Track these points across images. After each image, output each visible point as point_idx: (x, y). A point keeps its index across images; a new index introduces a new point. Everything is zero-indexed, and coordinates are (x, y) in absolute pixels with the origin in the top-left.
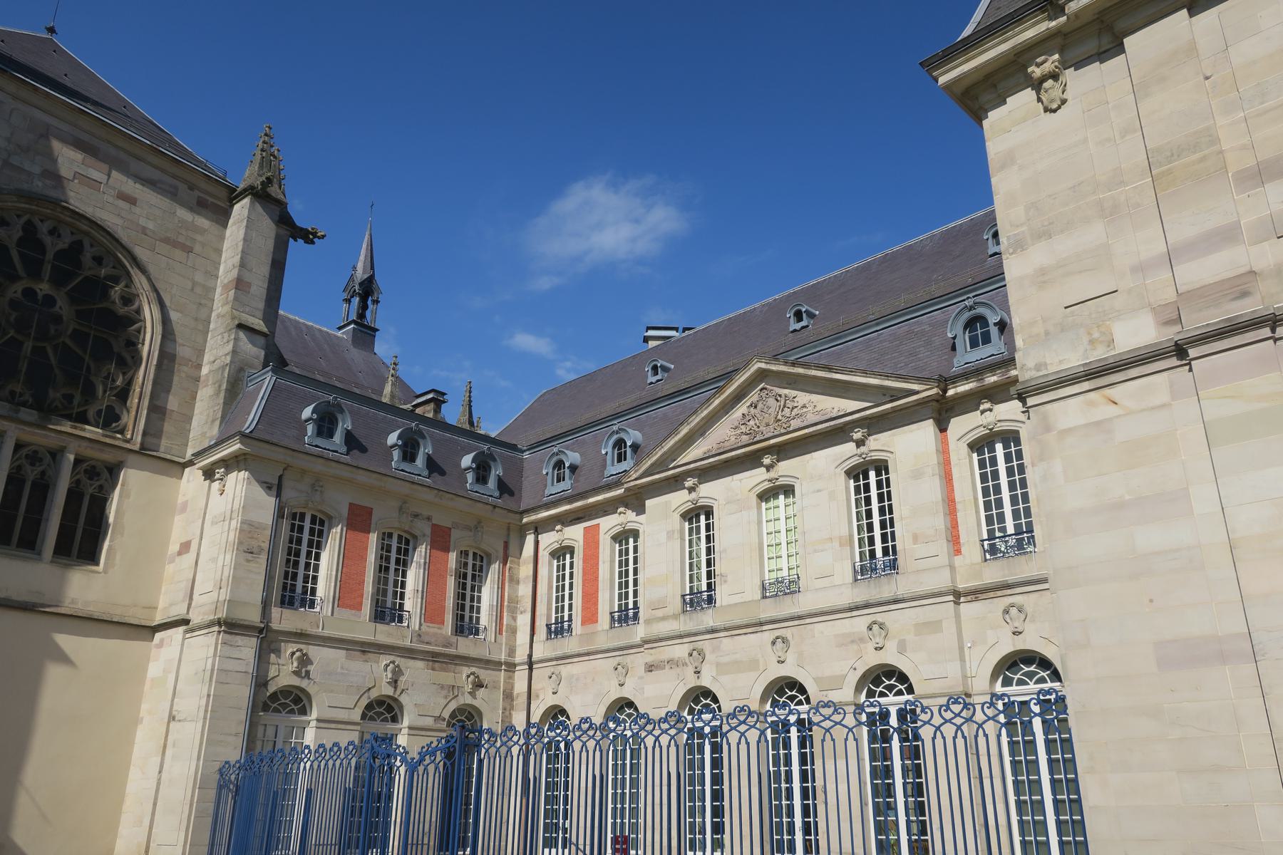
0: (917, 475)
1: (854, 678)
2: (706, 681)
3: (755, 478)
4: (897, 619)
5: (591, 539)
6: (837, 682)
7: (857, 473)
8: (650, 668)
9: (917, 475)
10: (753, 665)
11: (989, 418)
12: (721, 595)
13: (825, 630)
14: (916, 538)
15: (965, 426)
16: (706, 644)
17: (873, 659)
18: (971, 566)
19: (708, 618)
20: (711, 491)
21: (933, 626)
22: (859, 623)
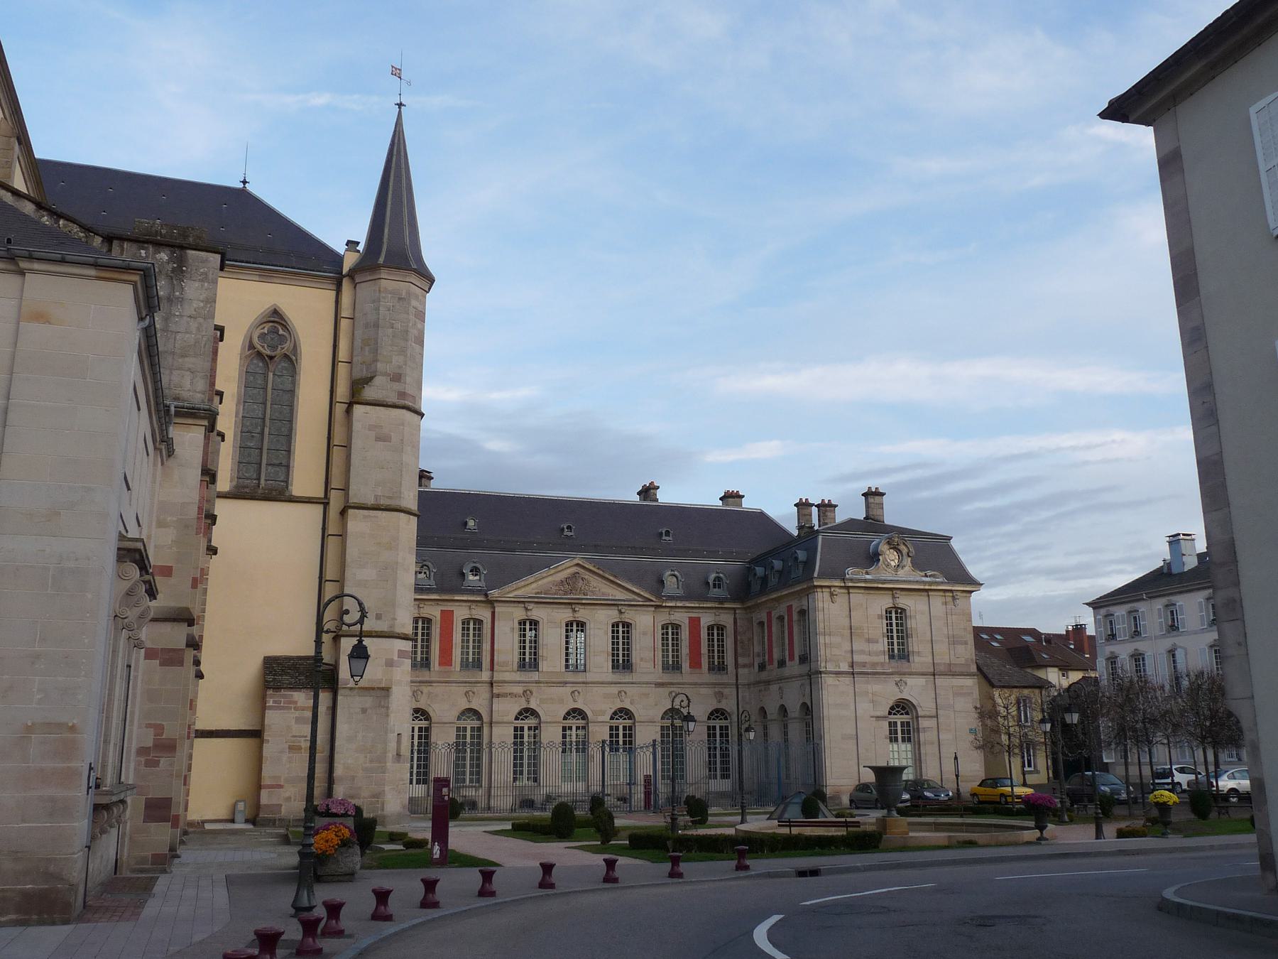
0: (645, 634)
1: (610, 712)
2: (533, 705)
3: (565, 615)
4: (629, 689)
5: (447, 617)
6: (603, 713)
7: (615, 625)
8: (498, 696)
9: (645, 634)
10: (561, 701)
11: (672, 617)
12: (543, 666)
13: (599, 691)
14: (642, 659)
15: (664, 618)
16: (533, 688)
17: (619, 705)
18: (658, 675)
19: (535, 676)
20: (537, 613)
21: (646, 695)
22: (614, 690)
